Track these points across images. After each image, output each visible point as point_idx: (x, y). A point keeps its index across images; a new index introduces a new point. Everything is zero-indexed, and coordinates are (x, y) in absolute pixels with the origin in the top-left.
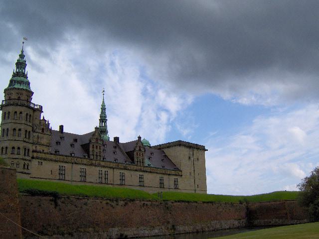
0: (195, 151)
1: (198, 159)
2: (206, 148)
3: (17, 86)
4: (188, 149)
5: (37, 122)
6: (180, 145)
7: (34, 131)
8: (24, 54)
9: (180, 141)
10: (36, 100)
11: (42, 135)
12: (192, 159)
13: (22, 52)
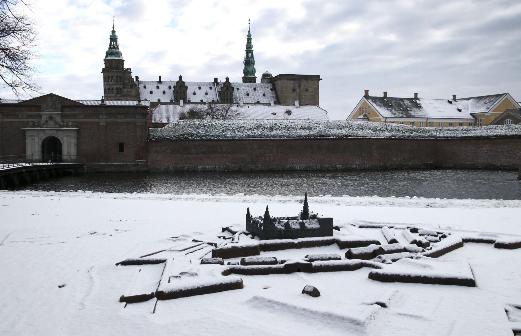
0: (304, 82)
1: (307, 90)
2: (320, 78)
3: (109, 58)
4: (292, 82)
5: (127, 81)
6: (280, 79)
7: (124, 87)
8: (115, 29)
9: (280, 75)
10: (126, 66)
11: (131, 90)
12: (298, 90)
13: (113, 28)
